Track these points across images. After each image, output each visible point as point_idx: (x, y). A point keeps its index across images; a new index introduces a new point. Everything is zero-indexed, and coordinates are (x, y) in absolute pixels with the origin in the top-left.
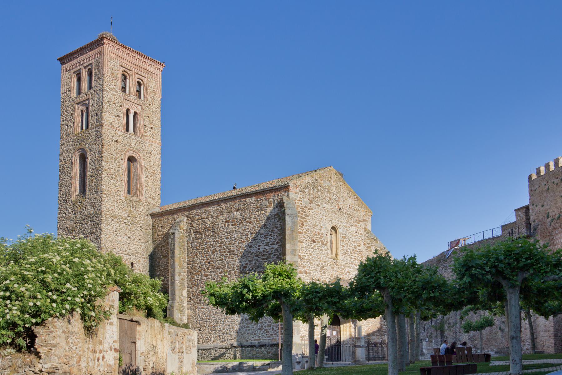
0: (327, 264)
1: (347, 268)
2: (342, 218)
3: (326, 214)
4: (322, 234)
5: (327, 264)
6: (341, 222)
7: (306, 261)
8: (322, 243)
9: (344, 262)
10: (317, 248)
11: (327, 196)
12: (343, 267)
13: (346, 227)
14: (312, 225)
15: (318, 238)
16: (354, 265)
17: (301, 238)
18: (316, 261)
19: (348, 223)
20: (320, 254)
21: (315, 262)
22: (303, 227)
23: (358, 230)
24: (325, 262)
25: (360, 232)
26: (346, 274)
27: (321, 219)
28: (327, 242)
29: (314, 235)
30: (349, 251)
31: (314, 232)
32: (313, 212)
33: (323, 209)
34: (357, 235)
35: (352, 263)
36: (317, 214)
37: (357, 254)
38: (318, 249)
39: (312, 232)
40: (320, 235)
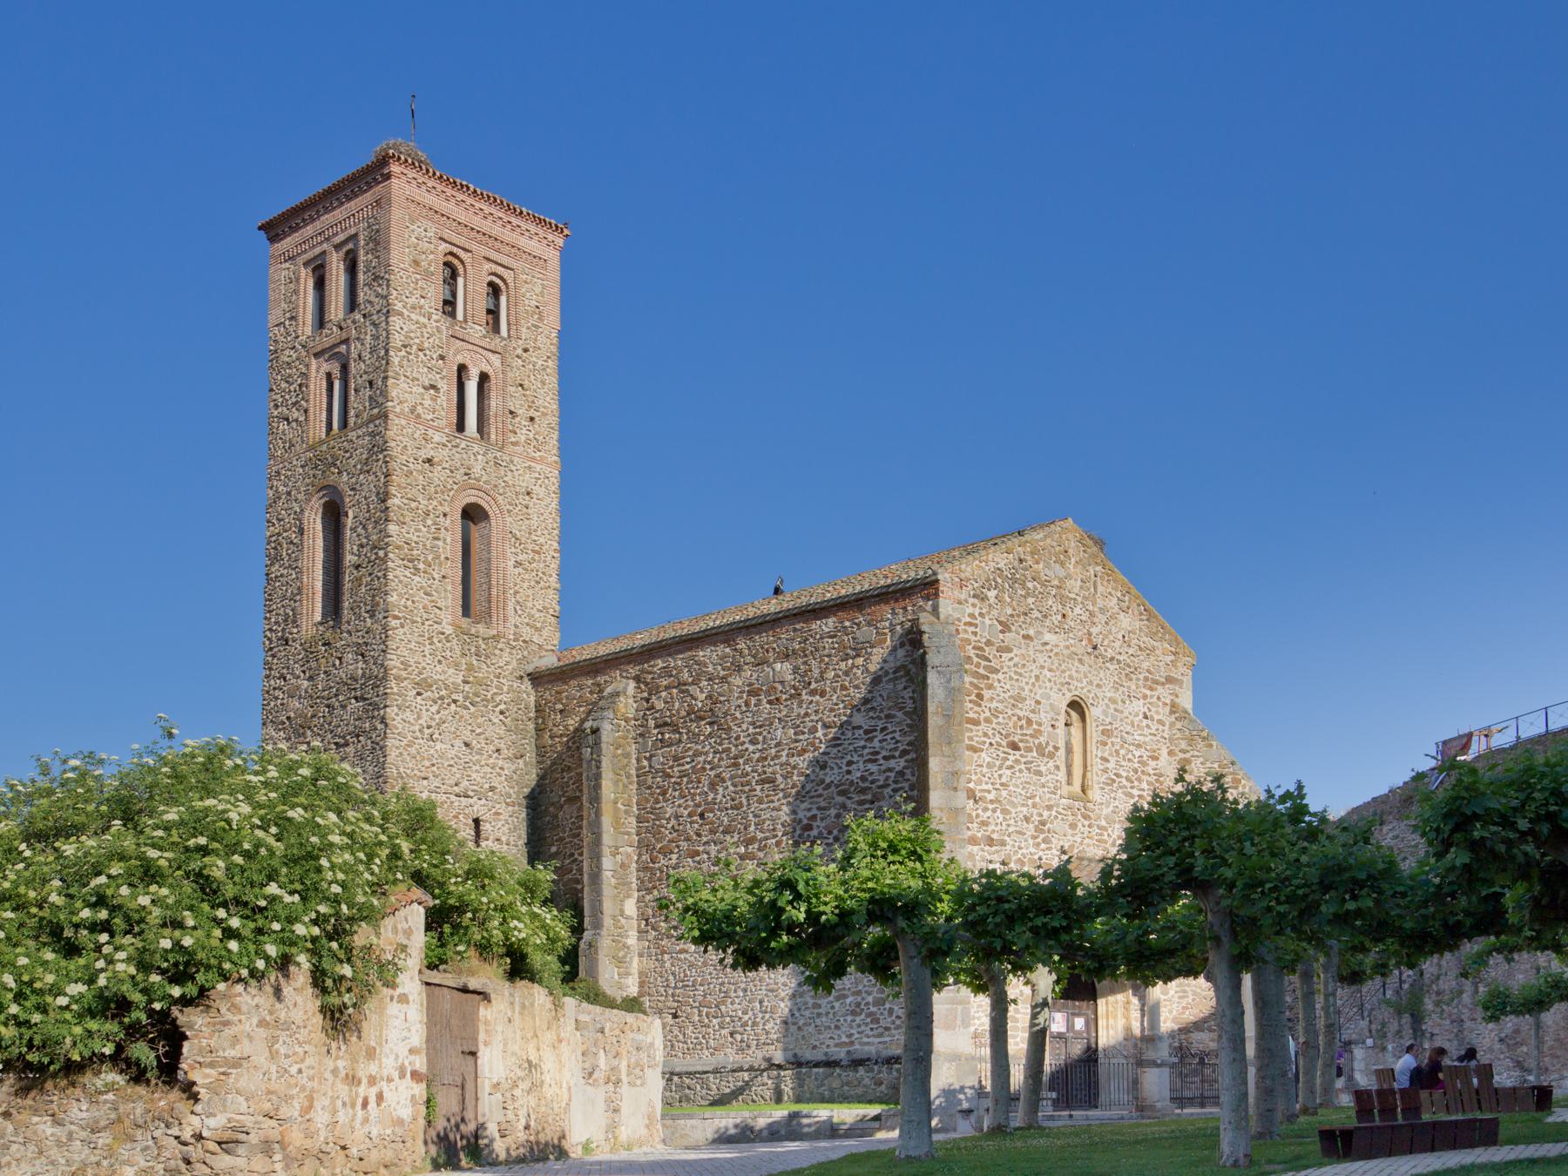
0: (1054, 813)
2: (1102, 675)
7: (991, 807)
8: (1041, 750)
9: (1107, 807)
10: (1023, 767)
12: (1103, 823)
17: (976, 739)
19: (1121, 689)
20: (1035, 784)
21: (1019, 809)
22: (980, 705)
24: (1049, 808)
25: (1156, 717)
27: (1037, 678)
28: (1056, 748)
29: (1015, 727)
30: (1124, 774)
32: (1011, 659)
33: (1041, 648)
34: (1148, 726)
36: (1024, 665)
38: (1028, 769)
40: (1035, 726)
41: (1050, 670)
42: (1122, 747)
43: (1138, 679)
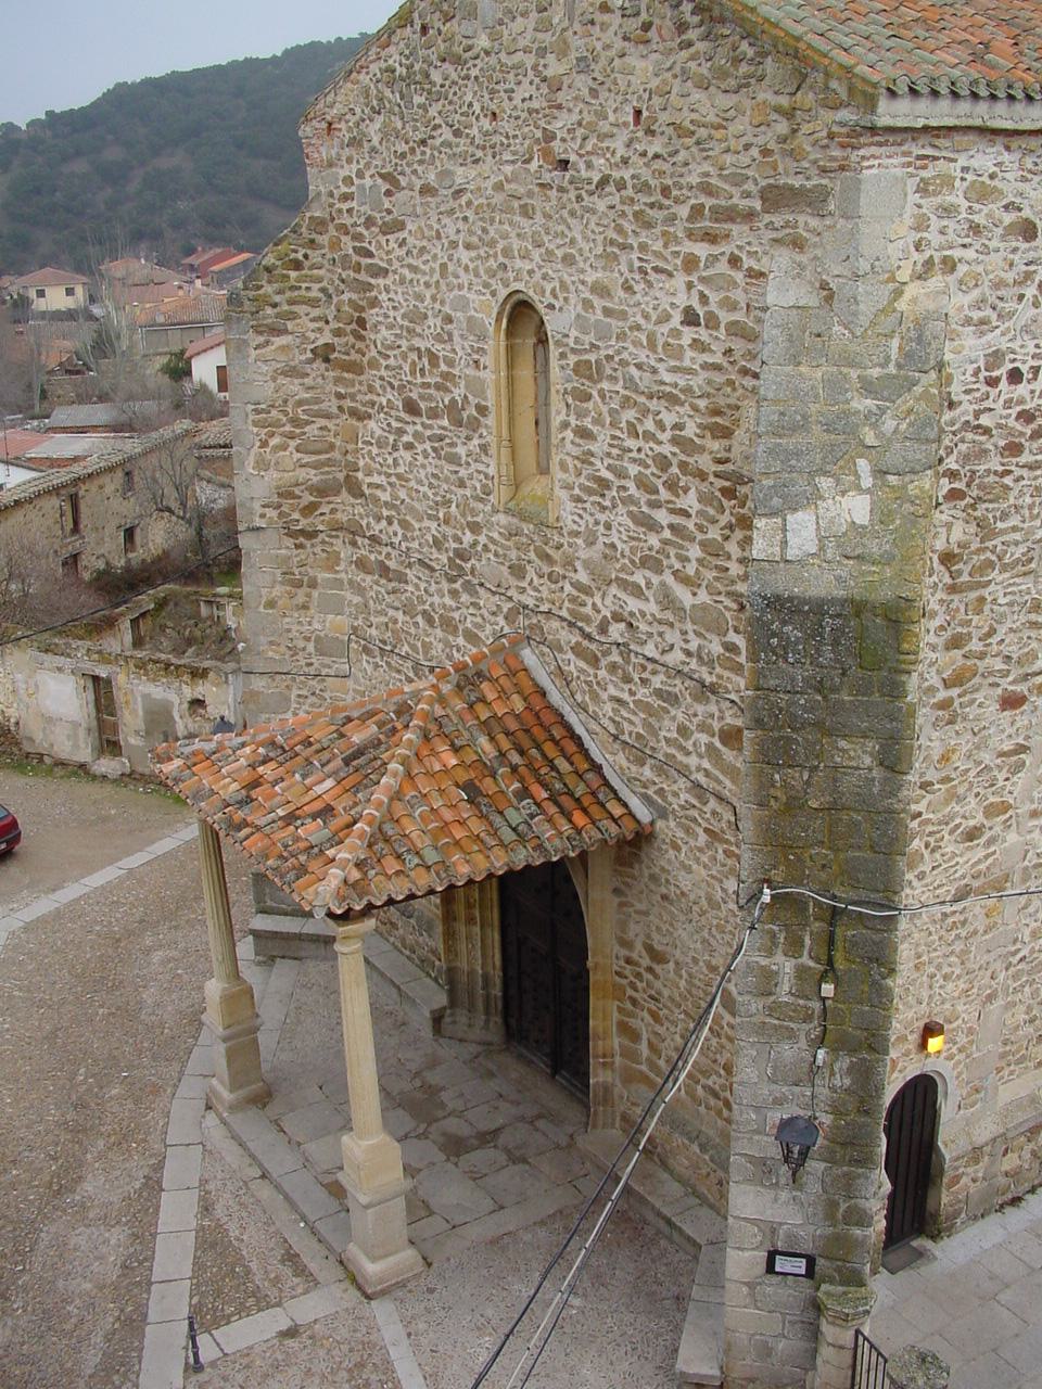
1: (614, 590)
3: (471, 232)
4: (451, 363)
5: (482, 539)
6: (568, 260)
7: (385, 513)
9: (591, 543)
10: (428, 446)
11: (477, 107)
12: (583, 576)
13: (601, 290)
14: (404, 316)
15: (432, 391)
16: (669, 579)
18: (430, 517)
20: (447, 480)
21: (427, 523)
23: (704, 299)
24: (475, 528)
25: (725, 317)
26: (603, 629)
28: (482, 410)
29: (413, 373)
33: (452, 204)
34: (697, 345)
35: (651, 563)
36: (423, 250)
38: (435, 450)
39: (405, 357)
40: (443, 367)
41: (468, 247)
42: (626, 402)
43: (672, 219)
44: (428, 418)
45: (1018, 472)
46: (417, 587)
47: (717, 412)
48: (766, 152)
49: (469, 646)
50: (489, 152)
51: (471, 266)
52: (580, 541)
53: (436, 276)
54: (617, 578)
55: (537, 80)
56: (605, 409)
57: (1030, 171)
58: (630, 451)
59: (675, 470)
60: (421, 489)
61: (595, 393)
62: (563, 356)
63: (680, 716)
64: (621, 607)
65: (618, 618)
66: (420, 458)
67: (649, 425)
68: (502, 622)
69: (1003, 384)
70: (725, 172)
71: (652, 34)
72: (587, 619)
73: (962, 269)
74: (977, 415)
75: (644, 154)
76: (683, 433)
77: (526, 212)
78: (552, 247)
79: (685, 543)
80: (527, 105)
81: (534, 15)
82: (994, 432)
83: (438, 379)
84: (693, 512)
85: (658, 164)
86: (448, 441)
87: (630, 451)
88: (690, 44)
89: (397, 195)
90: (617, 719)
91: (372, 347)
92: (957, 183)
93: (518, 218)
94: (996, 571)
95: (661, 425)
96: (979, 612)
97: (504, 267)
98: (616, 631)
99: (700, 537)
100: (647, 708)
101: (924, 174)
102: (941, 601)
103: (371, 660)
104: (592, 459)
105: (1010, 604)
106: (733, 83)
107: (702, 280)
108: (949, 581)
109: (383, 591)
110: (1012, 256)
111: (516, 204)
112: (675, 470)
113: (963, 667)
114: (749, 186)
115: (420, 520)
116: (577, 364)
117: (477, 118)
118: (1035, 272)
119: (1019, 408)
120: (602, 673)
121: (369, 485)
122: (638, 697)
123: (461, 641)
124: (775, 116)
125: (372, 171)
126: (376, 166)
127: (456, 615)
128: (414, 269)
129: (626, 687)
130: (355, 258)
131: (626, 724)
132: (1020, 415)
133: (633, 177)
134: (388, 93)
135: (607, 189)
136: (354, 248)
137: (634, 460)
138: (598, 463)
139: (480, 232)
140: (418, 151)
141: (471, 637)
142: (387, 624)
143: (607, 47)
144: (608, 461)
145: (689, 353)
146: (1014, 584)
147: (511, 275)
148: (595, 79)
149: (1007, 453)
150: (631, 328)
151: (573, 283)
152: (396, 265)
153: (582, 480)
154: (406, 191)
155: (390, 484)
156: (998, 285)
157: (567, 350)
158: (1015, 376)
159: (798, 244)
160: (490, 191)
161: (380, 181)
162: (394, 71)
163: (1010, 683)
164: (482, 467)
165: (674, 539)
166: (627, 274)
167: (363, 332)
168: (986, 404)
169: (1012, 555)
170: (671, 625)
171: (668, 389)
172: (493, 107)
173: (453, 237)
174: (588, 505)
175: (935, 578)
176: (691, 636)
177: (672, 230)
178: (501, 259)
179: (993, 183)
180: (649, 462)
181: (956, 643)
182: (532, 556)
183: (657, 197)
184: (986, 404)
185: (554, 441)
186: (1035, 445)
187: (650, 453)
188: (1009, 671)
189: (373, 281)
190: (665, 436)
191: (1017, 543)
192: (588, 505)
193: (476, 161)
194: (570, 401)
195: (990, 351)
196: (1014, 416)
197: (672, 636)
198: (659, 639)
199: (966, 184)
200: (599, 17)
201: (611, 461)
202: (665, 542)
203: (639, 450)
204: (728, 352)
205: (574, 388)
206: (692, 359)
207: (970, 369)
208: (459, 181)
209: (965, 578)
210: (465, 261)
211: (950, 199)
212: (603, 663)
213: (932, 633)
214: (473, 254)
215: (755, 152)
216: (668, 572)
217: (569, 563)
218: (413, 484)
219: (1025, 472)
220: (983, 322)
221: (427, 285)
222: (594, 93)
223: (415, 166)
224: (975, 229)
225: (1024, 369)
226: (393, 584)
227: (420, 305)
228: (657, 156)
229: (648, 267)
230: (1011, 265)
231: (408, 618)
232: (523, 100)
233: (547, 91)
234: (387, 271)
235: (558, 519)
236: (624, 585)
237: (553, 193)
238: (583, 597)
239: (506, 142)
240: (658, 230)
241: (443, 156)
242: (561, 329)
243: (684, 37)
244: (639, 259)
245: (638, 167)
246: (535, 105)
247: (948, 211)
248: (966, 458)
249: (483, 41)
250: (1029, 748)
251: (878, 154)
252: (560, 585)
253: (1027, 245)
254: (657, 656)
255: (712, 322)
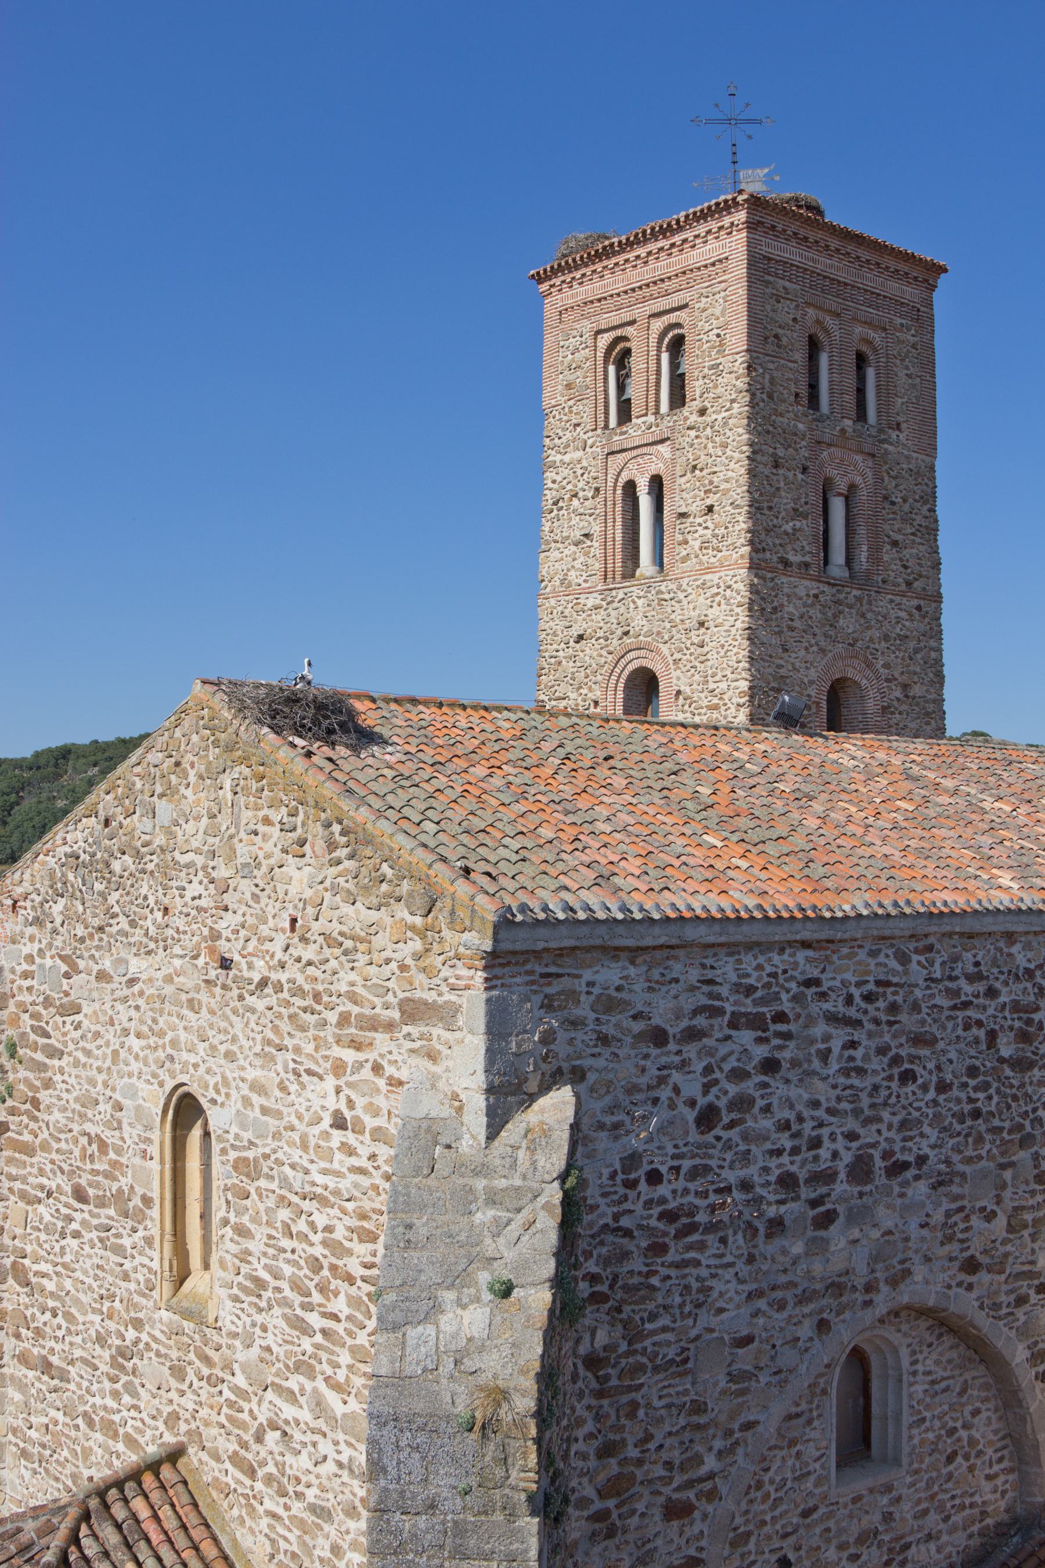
1: (270, 1395)
3: (142, 1022)
4: (119, 1151)
6: (230, 1056)
7: (51, 1303)
8: (120, 1198)
10: (94, 1234)
12: (240, 1381)
13: (258, 1088)
14: (77, 1099)
15: (100, 1178)
17: (31, 1180)
18: (94, 1311)
19: (280, 1057)
20: (112, 1272)
22: (35, 1119)
24: (138, 1324)
26: (259, 1439)
28: (147, 1201)
29: (83, 1158)
30: (288, 1270)
31: (84, 1140)
33: (126, 992)
35: (303, 1367)
36: (97, 1035)
37: (354, 1302)
38: (101, 1240)
40: (112, 1155)
41: (138, 1036)
43: (325, 1023)
44: (96, 1207)
45: (664, 1271)
46: (79, 1386)
47: (363, 1217)
48: (403, 968)
49: (129, 1453)
50: (161, 944)
51: (141, 1054)
52: (237, 1343)
53: (108, 1062)
54: (273, 1384)
55: (205, 881)
56: (262, 1207)
57: (657, 982)
58: (285, 1251)
59: (325, 1272)
60: (86, 1280)
61: (253, 1191)
62: (224, 1151)
63: (333, 1532)
64: (277, 1414)
65: (274, 1426)
66: (87, 1247)
67: (302, 1226)
68: (162, 1427)
69: (643, 1186)
70: (369, 983)
71: (307, 848)
72: (243, 1426)
73: (591, 1077)
74: (616, 1217)
75: (298, 960)
76: (333, 1236)
77: (193, 1006)
78: (215, 1041)
79: (337, 1349)
80: (197, 902)
81: (205, 820)
82: (636, 1233)
83: (107, 1167)
84: (342, 1316)
85: (311, 970)
86: (113, 1231)
87: (285, 1251)
88: (339, 862)
89: (75, 977)
90: (273, 1536)
91: (44, 1128)
92: (583, 998)
93: (185, 1012)
94: (649, 1374)
95: (312, 1225)
96: (632, 1415)
97: (171, 1058)
98: (272, 1437)
99: (349, 1342)
100: (301, 1523)
101: (549, 990)
102: (589, 1408)
103: (30, 1465)
104: (250, 1258)
105: (669, 1406)
106: (375, 901)
107: (349, 1085)
108: (594, 1384)
109: (44, 1388)
110: (643, 1062)
111: (184, 997)
112: (325, 1272)
113: (619, 1476)
114: (390, 997)
115: (85, 1314)
116: (237, 1160)
117: (152, 911)
118: (668, 1075)
119: (660, 1209)
120: (259, 1486)
121: (36, 1274)
122: (293, 1512)
123: (120, 1447)
124: (409, 934)
125: (54, 952)
126: (57, 948)
127: (116, 1418)
128: (88, 1053)
129: (282, 1500)
130: (33, 1037)
131: (281, 1542)
132: (661, 1217)
133: (289, 981)
134: (71, 876)
135: (266, 991)
136: (32, 1027)
137: (288, 1261)
138: (254, 1261)
139: (150, 1022)
140: (96, 937)
141: (131, 1442)
142: (47, 1426)
143: (268, 856)
144: (264, 1260)
145: (338, 1156)
146: (670, 1386)
147: (178, 1067)
148: (257, 886)
149: (650, 1253)
150: (285, 1128)
151: (234, 1079)
152: (71, 1047)
153: (240, 1278)
154: (83, 975)
155: (56, 1273)
156: (632, 1089)
157: (228, 1145)
158: (654, 1178)
159: (432, 1056)
160: (160, 983)
161: (59, 961)
162: (78, 858)
163: (678, 1489)
164: (146, 1261)
165: (325, 1343)
166: (283, 1074)
167: (36, 1113)
168: (626, 1206)
169: (664, 1356)
170: (325, 1435)
171: (319, 1190)
172: (166, 901)
173: (127, 1025)
174: (245, 1306)
175: (580, 1384)
176: (343, 1447)
177: (322, 1034)
178: (169, 1051)
179: (619, 995)
180: (302, 1263)
181: (607, 1451)
182: (192, 1356)
183: (309, 1002)
184: (626, 1206)
185: (214, 1239)
186: (681, 1244)
187: (303, 1255)
188: (671, 1478)
189: (47, 1061)
190: (316, 1238)
191: (668, 1343)
192: (245, 1306)
193: (149, 953)
194: (230, 1197)
195: (626, 1154)
196: (656, 1216)
197: (325, 1447)
198: (312, 1450)
199: (592, 998)
200: (261, 828)
201: (268, 1261)
202: (317, 1346)
203: (293, 1251)
204: (373, 1157)
205: (233, 1184)
206: (341, 1162)
207: (606, 1172)
208: (132, 970)
209: (614, 1382)
210: (136, 1049)
211: (578, 1012)
212: (260, 1473)
213: (581, 1440)
214: (143, 1042)
215: (394, 965)
216: (320, 1378)
217: (228, 1367)
218: (78, 1274)
219: (673, 1272)
220: (616, 1126)
221: (99, 1070)
222: (255, 897)
223: (93, 951)
224: (604, 1040)
225: (664, 1169)
226: (56, 1382)
227: (92, 1090)
228: (310, 963)
229: (302, 1068)
230: (643, 1070)
231: (68, 1420)
232: (193, 899)
233: (213, 892)
234: (62, 1053)
235: (216, 1320)
236: (279, 1389)
237: (218, 990)
238: (241, 1403)
239: (176, 936)
240: (310, 1034)
241: (118, 944)
242: (222, 1125)
243: (334, 855)
244: (294, 1061)
245: (293, 971)
246: (203, 903)
247: (575, 1024)
248: (606, 1262)
249: (160, 840)
250: (703, 1561)
251: (500, 974)
252: (218, 1388)
253: (658, 1051)
254: (311, 1468)
255: (359, 1129)
